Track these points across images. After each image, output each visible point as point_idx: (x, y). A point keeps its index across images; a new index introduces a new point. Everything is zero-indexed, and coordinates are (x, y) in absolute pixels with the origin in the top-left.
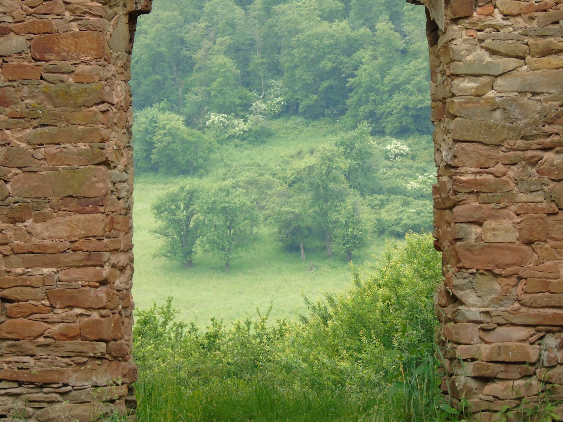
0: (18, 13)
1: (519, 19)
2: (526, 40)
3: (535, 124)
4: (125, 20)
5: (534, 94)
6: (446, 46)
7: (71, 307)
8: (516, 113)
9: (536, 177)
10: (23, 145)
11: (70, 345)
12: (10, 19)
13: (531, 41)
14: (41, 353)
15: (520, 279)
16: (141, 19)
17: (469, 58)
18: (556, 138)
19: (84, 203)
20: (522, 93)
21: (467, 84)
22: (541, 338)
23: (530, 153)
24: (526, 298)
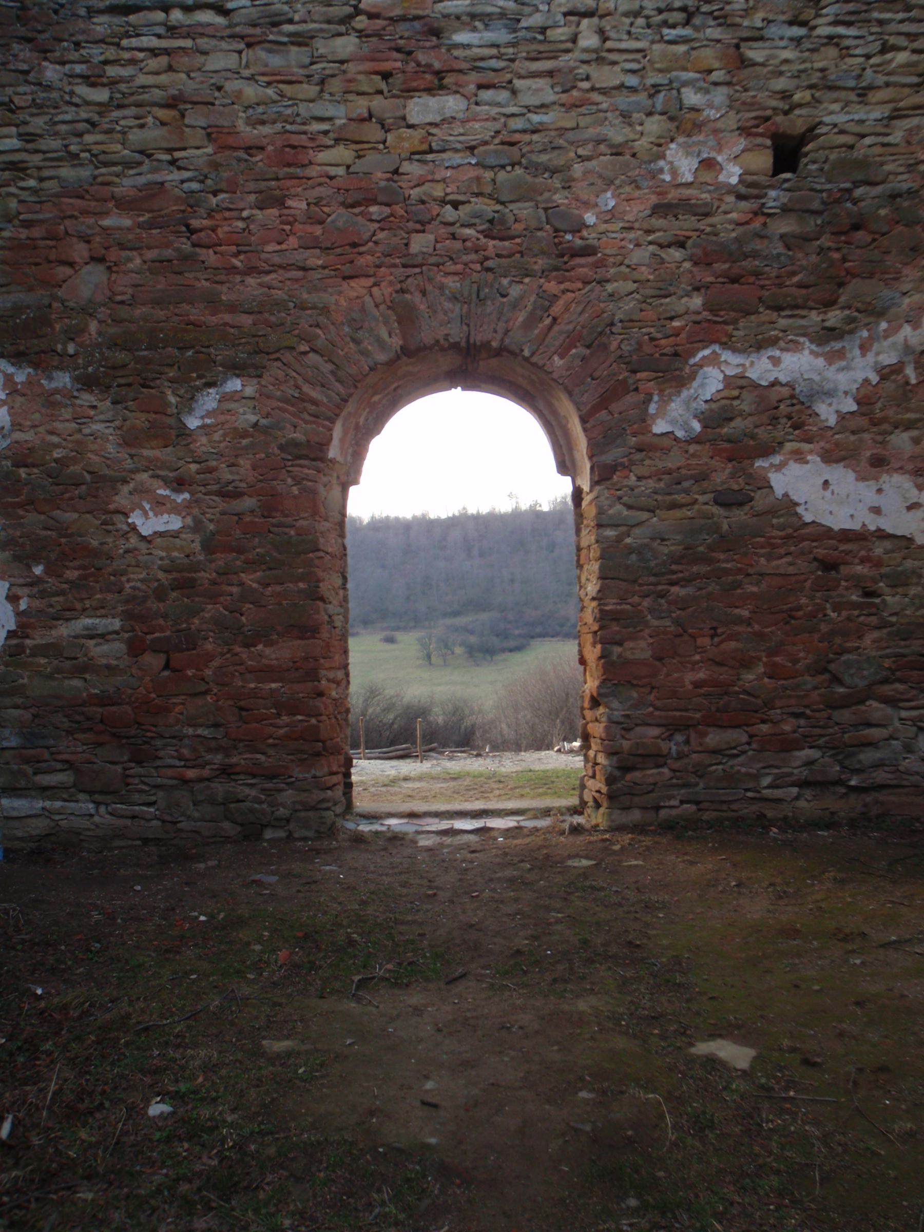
1: (650, 481)
2: (656, 497)
5: (663, 540)
7: (295, 715)
9: (665, 606)
10: (255, 585)
12: (244, 485)
13: (659, 498)
14: (271, 752)
15: (653, 688)
17: (611, 512)
18: (680, 575)
20: (653, 539)
22: (671, 735)
23: (660, 588)
24: (658, 703)
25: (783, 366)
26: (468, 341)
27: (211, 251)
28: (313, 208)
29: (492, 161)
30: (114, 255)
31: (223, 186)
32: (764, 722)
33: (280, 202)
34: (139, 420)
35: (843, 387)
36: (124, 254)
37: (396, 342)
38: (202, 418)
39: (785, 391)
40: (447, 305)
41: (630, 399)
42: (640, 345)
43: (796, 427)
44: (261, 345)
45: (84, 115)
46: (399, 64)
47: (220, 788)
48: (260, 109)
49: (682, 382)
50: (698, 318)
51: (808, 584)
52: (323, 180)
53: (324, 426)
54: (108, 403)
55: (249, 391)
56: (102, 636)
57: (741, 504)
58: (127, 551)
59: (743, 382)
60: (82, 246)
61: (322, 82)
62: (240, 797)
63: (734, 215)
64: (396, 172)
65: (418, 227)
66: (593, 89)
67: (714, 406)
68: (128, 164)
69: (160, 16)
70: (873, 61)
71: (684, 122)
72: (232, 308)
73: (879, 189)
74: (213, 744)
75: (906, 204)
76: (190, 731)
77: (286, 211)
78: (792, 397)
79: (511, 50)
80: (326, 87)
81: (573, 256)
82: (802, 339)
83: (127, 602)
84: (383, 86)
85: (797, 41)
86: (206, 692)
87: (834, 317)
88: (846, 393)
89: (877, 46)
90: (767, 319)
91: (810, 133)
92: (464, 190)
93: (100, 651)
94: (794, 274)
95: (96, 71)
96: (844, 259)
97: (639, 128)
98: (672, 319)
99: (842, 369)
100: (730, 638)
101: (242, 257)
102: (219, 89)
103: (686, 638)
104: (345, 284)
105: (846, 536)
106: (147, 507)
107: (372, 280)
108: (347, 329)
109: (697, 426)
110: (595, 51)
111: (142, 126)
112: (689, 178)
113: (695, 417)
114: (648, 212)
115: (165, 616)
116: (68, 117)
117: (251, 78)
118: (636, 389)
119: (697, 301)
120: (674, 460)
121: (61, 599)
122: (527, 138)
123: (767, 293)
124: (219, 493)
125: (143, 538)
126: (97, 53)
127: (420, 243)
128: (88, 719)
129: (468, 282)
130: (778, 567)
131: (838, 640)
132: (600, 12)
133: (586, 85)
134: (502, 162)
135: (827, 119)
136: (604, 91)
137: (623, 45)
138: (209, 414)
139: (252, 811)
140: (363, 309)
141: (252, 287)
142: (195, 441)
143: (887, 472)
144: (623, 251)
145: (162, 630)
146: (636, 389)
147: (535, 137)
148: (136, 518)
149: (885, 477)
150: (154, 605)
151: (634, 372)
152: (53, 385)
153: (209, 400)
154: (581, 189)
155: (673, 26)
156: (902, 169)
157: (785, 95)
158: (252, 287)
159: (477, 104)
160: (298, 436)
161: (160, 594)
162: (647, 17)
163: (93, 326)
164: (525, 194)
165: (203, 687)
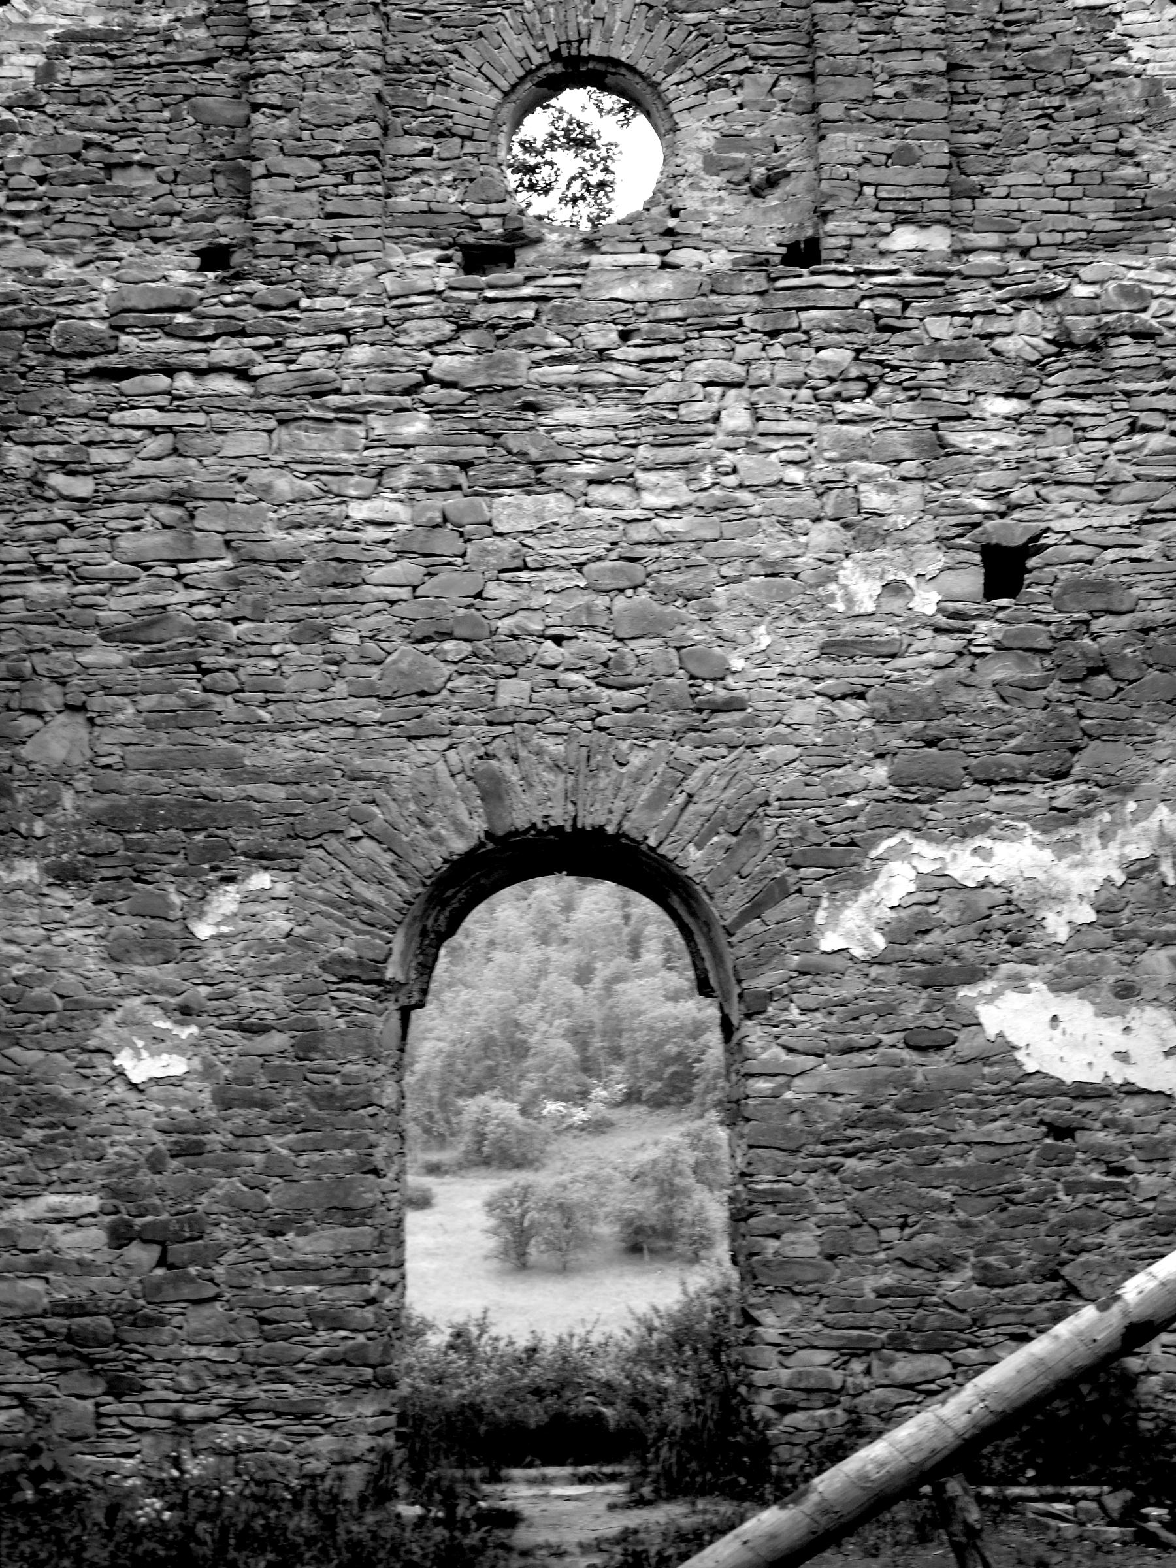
0: (281, 1008)
3: (835, 1127)
4: (396, 1016)
5: (836, 1095)
6: (739, 1044)
7: (335, 1329)
8: (816, 1116)
9: (838, 1185)
10: (285, 1152)
11: (333, 1371)
14: (302, 1380)
15: (822, 1296)
16: (415, 1014)
17: (765, 1056)
18: (858, 1143)
19: (351, 1215)
20: (822, 1094)
21: (763, 1085)
22: (846, 1362)
23: (831, 1160)
24: (829, 1318)
25: (995, 860)
26: (574, 825)
27: (229, 699)
28: (372, 645)
29: (607, 583)
30: (97, 702)
31: (247, 612)
32: (973, 1345)
33: (323, 634)
34: (129, 926)
35: (1078, 889)
36: (110, 700)
37: (478, 826)
38: (217, 924)
39: (1000, 895)
40: (548, 776)
41: (791, 904)
42: (804, 830)
43: (1013, 944)
44: (298, 828)
45: (59, 514)
46: (482, 451)
47: (231, 1434)
48: (297, 508)
49: (860, 882)
50: (882, 794)
51: (1032, 1156)
52: (379, 606)
53: (381, 937)
54: (88, 903)
55: (281, 889)
56: (73, 1220)
57: (940, 1048)
58: (110, 1105)
59: (942, 882)
60: (55, 689)
61: (379, 474)
62: (257, 1444)
63: (930, 656)
64: (478, 595)
65: (509, 671)
66: (741, 486)
67: (903, 914)
68: (118, 582)
69: (162, 381)
70: (1117, 446)
71: (864, 531)
72: (258, 776)
73: (1127, 619)
74: (223, 1370)
75: (1162, 641)
76: (192, 1351)
77: (331, 647)
78: (1009, 902)
79: (631, 433)
80: (386, 480)
81: (714, 711)
82: (1021, 825)
83: (110, 1173)
84: (462, 479)
85: (1016, 419)
86: (215, 1298)
87: (1066, 794)
88: (1081, 897)
89: (1124, 426)
90: (974, 796)
91: (1033, 546)
92: (569, 621)
93: (68, 1240)
94: (1011, 735)
95: (78, 456)
96: (1080, 716)
97: (803, 539)
98: (846, 795)
99: (1075, 866)
100: (925, 1230)
101: (271, 708)
102: (241, 480)
103: (866, 1229)
104: (410, 745)
105: (1082, 1092)
106: (140, 1044)
107: (447, 741)
108: (412, 807)
109: (880, 942)
110: (747, 434)
111: (137, 529)
112: (869, 607)
113: (878, 929)
114: (816, 653)
115: (161, 1193)
116: (37, 516)
117: (284, 466)
118: (799, 891)
119: (880, 772)
120: (852, 986)
121: (17, 1168)
122: (654, 551)
123: (974, 762)
124: (240, 1027)
125: (134, 1086)
126: (78, 431)
127: (512, 692)
128: (49, 1334)
129: (575, 745)
130: (990, 1133)
131: (1073, 1234)
132: (753, 382)
133: (732, 480)
134: (621, 585)
135: (1056, 525)
136: (754, 489)
137: (782, 427)
138: (226, 919)
139: (273, 1464)
140: (435, 781)
141: (283, 751)
142: (206, 956)
143: (1137, 1004)
144: (782, 706)
145: (156, 1210)
146: (799, 891)
147: (664, 551)
148: (124, 1059)
149: (1134, 1011)
150: (145, 1177)
151: (796, 867)
152: (15, 877)
153: (226, 901)
154: (726, 623)
155: (849, 400)
156: (1156, 594)
157: (999, 493)
158: (283, 751)
159: (587, 505)
160: (346, 950)
161: (156, 1164)
162: (814, 388)
163: (68, 799)
164: (650, 628)
165: (211, 1291)
